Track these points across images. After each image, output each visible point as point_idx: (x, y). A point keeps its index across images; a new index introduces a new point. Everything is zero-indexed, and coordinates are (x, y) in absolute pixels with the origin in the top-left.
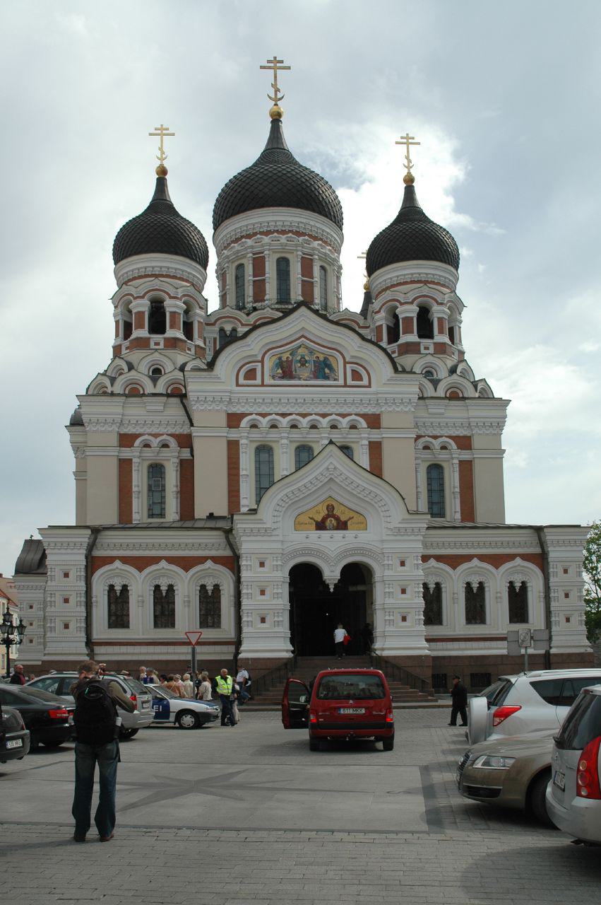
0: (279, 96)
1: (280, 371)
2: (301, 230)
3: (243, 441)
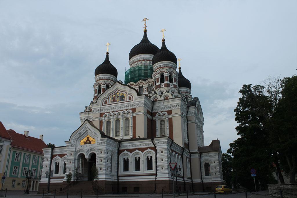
0: (146, 26)
1: (113, 100)
2: (144, 59)
3: (103, 120)
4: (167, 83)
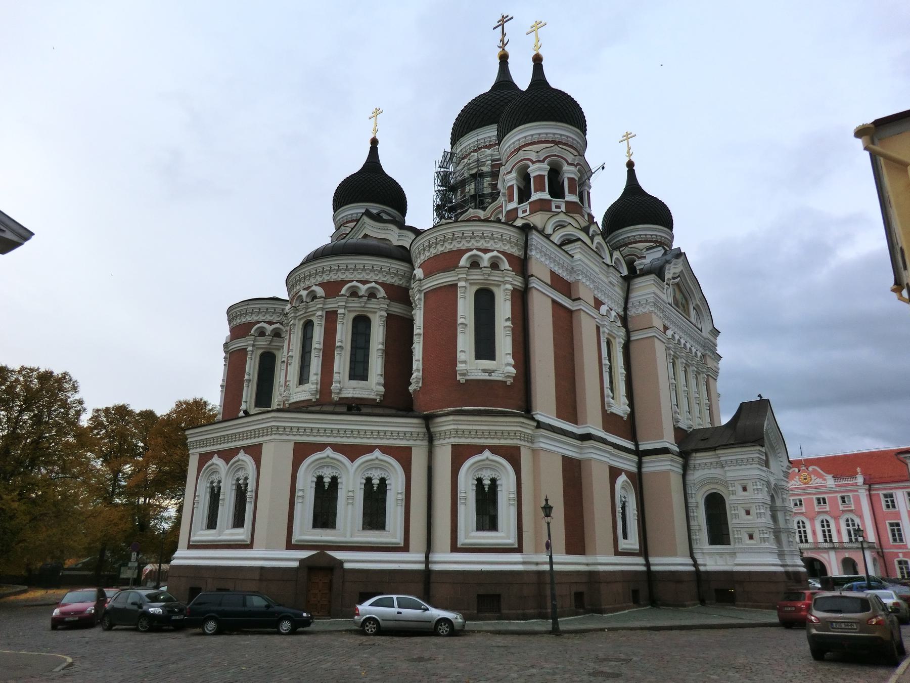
4: (540, 200)
